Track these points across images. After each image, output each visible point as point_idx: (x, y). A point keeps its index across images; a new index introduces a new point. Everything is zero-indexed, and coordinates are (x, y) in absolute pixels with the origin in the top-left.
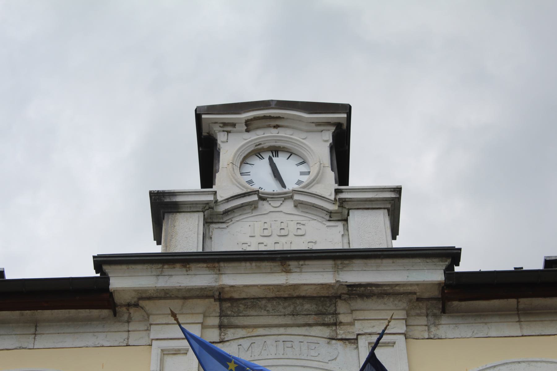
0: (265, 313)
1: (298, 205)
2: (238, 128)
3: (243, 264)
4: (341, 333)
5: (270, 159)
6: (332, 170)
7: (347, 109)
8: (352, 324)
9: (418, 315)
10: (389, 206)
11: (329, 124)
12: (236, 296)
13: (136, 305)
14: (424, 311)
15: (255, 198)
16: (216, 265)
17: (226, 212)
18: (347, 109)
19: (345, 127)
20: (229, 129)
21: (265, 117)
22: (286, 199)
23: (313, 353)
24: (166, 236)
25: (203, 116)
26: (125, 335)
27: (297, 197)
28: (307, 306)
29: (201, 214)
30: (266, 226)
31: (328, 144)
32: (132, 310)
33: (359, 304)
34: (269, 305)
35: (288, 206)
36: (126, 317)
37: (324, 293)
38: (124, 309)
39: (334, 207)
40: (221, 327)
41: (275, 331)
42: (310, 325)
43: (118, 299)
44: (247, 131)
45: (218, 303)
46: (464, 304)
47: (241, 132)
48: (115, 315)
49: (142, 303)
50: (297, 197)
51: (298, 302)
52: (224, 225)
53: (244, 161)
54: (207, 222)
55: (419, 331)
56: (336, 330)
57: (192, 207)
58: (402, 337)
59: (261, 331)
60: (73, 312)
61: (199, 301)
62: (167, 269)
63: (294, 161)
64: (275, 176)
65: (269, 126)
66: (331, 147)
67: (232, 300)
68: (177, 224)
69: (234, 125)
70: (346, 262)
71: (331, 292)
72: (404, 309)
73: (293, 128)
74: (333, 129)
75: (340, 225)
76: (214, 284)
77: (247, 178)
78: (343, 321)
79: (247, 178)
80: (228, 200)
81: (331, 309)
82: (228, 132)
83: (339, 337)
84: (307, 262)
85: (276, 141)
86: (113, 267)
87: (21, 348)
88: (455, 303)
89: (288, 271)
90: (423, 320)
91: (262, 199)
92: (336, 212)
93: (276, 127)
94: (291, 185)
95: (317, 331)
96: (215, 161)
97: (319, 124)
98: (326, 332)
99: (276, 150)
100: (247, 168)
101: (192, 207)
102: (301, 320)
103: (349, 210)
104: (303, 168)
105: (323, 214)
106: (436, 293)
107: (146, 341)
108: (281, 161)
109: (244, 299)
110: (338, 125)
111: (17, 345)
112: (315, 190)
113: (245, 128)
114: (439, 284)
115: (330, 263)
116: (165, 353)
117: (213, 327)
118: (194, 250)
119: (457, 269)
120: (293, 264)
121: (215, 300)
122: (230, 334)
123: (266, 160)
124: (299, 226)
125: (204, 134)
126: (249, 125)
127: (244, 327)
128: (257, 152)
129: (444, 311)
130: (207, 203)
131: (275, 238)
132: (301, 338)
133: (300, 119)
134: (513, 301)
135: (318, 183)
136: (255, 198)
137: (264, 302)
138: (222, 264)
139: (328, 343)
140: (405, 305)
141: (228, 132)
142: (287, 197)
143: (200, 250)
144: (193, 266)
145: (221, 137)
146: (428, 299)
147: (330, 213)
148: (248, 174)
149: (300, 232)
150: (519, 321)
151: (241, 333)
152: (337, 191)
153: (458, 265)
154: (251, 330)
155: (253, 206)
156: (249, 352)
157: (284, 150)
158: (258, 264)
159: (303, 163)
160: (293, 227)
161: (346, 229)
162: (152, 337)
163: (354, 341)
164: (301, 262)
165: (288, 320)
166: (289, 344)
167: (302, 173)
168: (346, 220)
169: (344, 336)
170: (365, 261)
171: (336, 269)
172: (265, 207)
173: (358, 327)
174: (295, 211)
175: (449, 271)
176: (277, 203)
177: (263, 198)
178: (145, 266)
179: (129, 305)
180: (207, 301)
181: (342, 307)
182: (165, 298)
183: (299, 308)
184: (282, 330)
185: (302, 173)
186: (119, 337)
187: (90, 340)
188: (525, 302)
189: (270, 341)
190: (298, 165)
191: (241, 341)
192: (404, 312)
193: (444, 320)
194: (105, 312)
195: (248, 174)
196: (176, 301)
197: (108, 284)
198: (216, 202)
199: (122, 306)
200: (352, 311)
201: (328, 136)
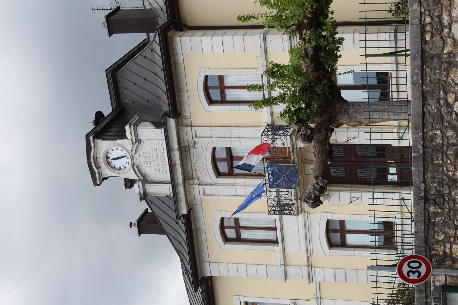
5: (112, 159)
35: (136, 156)
41: (193, 164)
44: (100, 168)
59: (193, 167)
65: (97, 160)
69: (99, 173)
74: (96, 140)
82: (102, 174)
85: (104, 158)
93: (97, 158)
97: (94, 145)
99: (107, 158)
116: (204, 195)
122: (195, 176)
126: (98, 167)
128: (109, 164)
149: (148, 152)
151: (194, 173)
177: (133, 164)
184: (192, 162)
189: (196, 165)
197: (185, 214)
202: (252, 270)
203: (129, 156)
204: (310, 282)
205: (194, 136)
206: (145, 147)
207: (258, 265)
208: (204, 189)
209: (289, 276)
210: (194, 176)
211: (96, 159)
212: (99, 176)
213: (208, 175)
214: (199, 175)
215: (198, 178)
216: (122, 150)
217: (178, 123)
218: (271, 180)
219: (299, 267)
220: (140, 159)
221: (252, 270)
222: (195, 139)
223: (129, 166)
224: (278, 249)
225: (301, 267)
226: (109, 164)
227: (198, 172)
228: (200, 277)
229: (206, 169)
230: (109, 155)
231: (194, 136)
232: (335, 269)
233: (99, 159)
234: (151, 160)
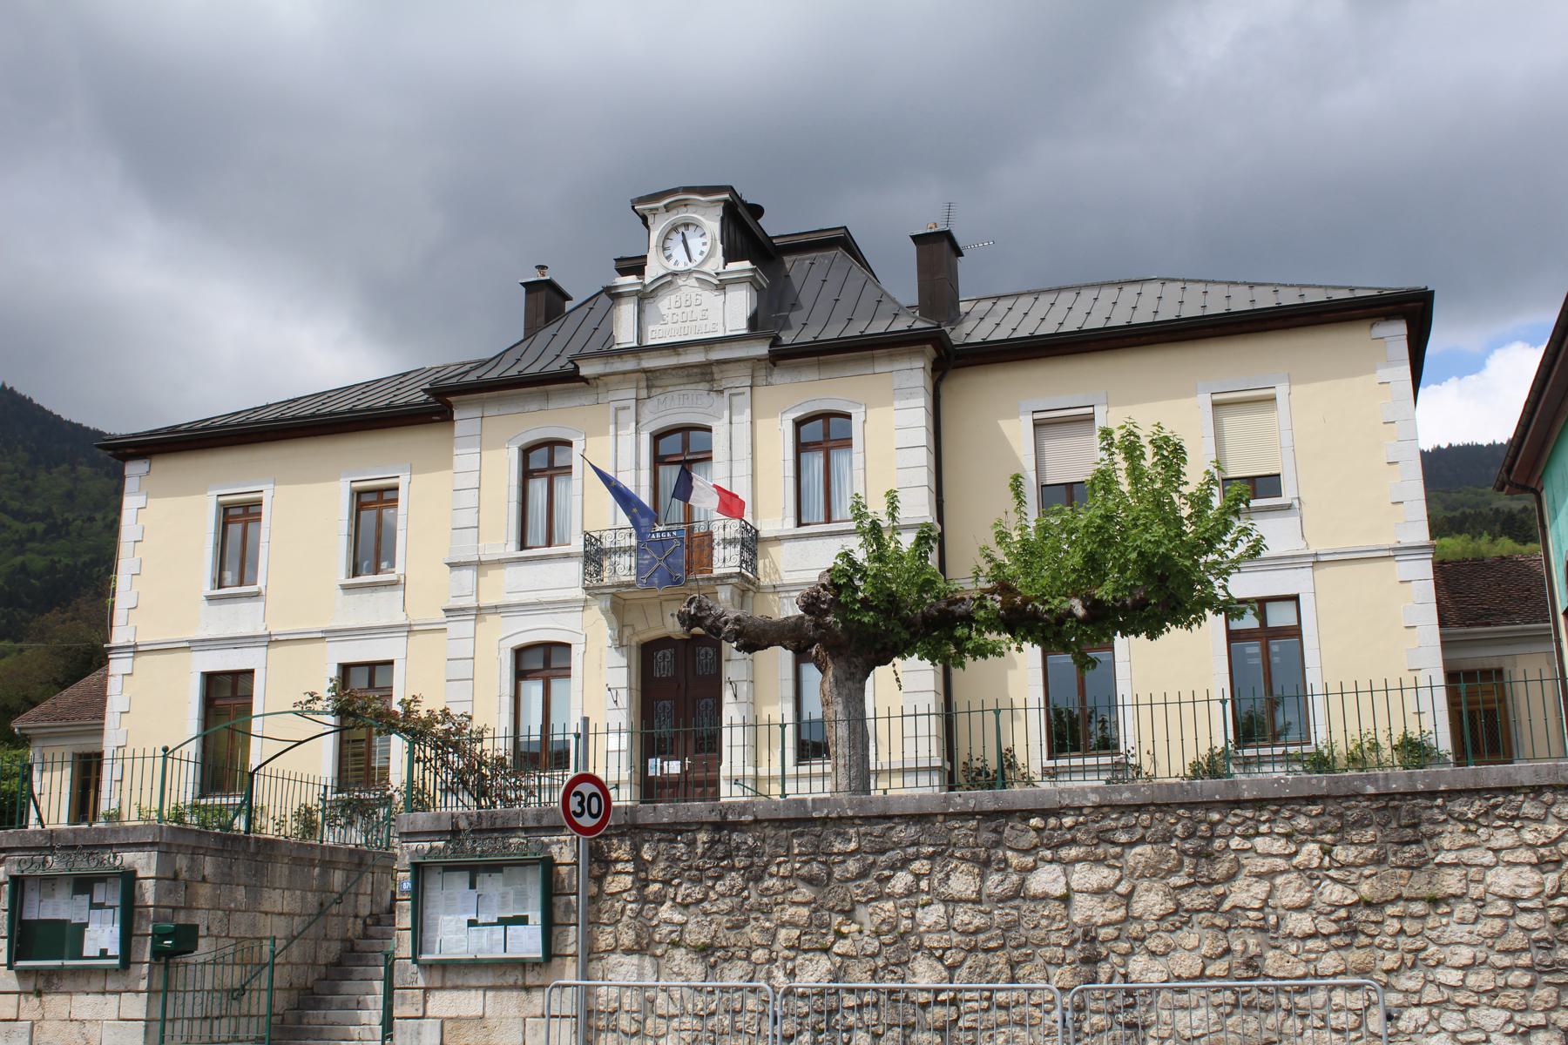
1: (697, 279)
5: (683, 233)
6: (722, 243)
11: (718, 201)
17: (653, 290)
29: (636, 298)
31: (719, 218)
35: (692, 282)
40: (649, 387)
41: (678, 388)
44: (667, 211)
52: (651, 300)
59: (670, 389)
62: (610, 360)
63: (699, 232)
69: (657, 209)
74: (722, 204)
80: (652, 282)
89: (679, 354)
93: (686, 205)
99: (687, 225)
101: (630, 294)
104: (703, 240)
110: (725, 201)
112: (706, 268)
122: (654, 392)
126: (667, 208)
128: (675, 228)
137: (669, 371)
151: (659, 391)
155: (670, 283)
157: (693, 224)
160: (693, 295)
172: (680, 281)
177: (675, 274)
184: (682, 387)
185: (704, 244)
186: (592, 398)
189: (675, 395)
190: (701, 236)
194: (583, 384)
202: (469, 499)
203: (690, 266)
205: (734, 391)
206: (711, 299)
207: (478, 511)
208: (629, 408)
210: (653, 390)
211: (685, 204)
212: (651, 210)
213: (656, 416)
214: (655, 399)
215: (649, 398)
216: (702, 253)
217: (758, 360)
218: (653, 536)
220: (688, 287)
221: (469, 499)
222: (726, 393)
223: (671, 267)
224: (512, 550)
226: (675, 228)
227: (662, 398)
228: (450, 399)
229: (669, 412)
230: (692, 228)
231: (734, 391)
233: (684, 209)
234: (683, 309)
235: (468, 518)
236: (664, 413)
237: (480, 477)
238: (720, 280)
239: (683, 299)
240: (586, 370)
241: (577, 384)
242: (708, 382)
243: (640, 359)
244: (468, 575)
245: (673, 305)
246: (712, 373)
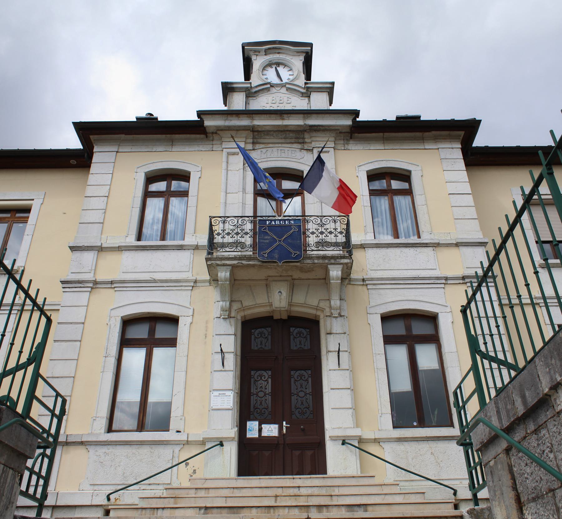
0: (273, 137)
1: (288, 89)
2: (261, 53)
3: (263, 115)
4: (306, 147)
5: (276, 68)
6: (304, 74)
7: (311, 45)
8: (311, 143)
9: (340, 139)
10: (329, 91)
11: (303, 52)
12: (260, 129)
13: (216, 133)
14: (343, 138)
15: (269, 86)
16: (251, 115)
17: (256, 92)
18: (311, 45)
19: (310, 54)
20: (257, 54)
21: (274, 48)
22: (282, 86)
23: (293, 155)
24: (229, 102)
25: (246, 47)
26: (211, 146)
27: (287, 86)
28: (291, 135)
29: (244, 93)
30: (273, 99)
31: (302, 62)
32: (214, 135)
33: (314, 134)
34: (275, 134)
35: (284, 90)
36: (211, 138)
37: (299, 129)
38: (211, 135)
39: (304, 91)
41: (277, 145)
42: (292, 143)
43: (208, 130)
44: (265, 55)
45: (252, 133)
46: (360, 135)
47: (262, 55)
48: (207, 137)
49: (218, 132)
50: (287, 86)
51: (287, 133)
52: (255, 98)
53: (264, 69)
54: (247, 97)
55: (339, 147)
56: (304, 146)
57: (240, 90)
58: (333, 149)
59: (271, 145)
60: (188, 135)
61: (244, 132)
62: (230, 117)
63: (286, 69)
64: (278, 76)
65: (275, 53)
66: (303, 63)
67: (258, 131)
68: (234, 97)
70: (309, 115)
71: (302, 129)
72: (334, 137)
73: (286, 54)
74: (304, 54)
75: (307, 99)
76: (250, 124)
77: (265, 77)
78: (307, 141)
79: (265, 77)
80: (257, 87)
81: (302, 136)
82: (257, 55)
83: (305, 148)
84: (291, 115)
85: (279, 60)
86: (206, 116)
87: (166, 151)
88: (356, 134)
89: (283, 119)
90: (342, 142)
91: (272, 86)
92: (305, 93)
93: (279, 53)
94: (285, 80)
95: (295, 146)
96: (251, 69)
98: (300, 146)
99: (278, 64)
100: (265, 72)
101: (240, 90)
102: (288, 141)
103: (311, 92)
104: (291, 73)
105: (299, 94)
106: (348, 130)
107: (221, 149)
108: (280, 69)
109: (264, 131)
110: (307, 53)
111: (165, 150)
112: (296, 83)
113: (265, 53)
114: (350, 126)
115: (302, 115)
116: (229, 154)
117: (250, 143)
118: (242, 109)
119: (358, 119)
120: (285, 116)
121: (251, 131)
122: (257, 146)
123: (274, 69)
124: (288, 99)
125: (246, 56)
126: (267, 52)
127: (263, 143)
128: (270, 65)
129: (351, 138)
130: (247, 88)
131: (277, 104)
132: (288, 149)
133: (290, 49)
134: (381, 134)
135: (297, 79)
136: (269, 86)
137: (272, 132)
138: (254, 115)
139: (300, 151)
140: (334, 135)
141: (257, 55)
142: (283, 86)
143: (244, 109)
144: (241, 116)
145: (253, 58)
146: (344, 133)
147: (302, 93)
148: (265, 75)
149: (289, 102)
150: (384, 143)
152: (306, 84)
153: (358, 118)
154: (266, 145)
155: (268, 90)
156: (266, 154)
158: (270, 115)
159: (291, 70)
160: (285, 99)
161: (309, 100)
162: (223, 147)
163: (311, 150)
164: (289, 115)
165: (283, 141)
166: (283, 151)
167: (290, 75)
168: (309, 97)
169: (307, 148)
170: (318, 115)
171: (304, 119)
172: (273, 90)
173: (313, 144)
174: (286, 92)
175: (354, 120)
176: (279, 89)
177: (272, 86)
178: (219, 116)
179: (213, 133)
180: (247, 132)
181: (306, 135)
182: (229, 130)
183: (288, 136)
184: (280, 145)
185: (290, 75)
186: (209, 147)
187: (197, 148)
188: (386, 135)
189: (275, 149)
190: (288, 71)
191: (262, 150)
192: (334, 138)
193: (351, 142)
195: (265, 75)
196: (234, 131)
197: (204, 123)
198: (251, 87)
199: (210, 133)
200: (311, 137)
201: (302, 58)
204: (63, 282)
207: (105, 213)
209: (78, 254)
211: (277, 51)
212: (255, 51)
214: (259, 151)
215: (254, 150)
219: (93, 268)
224: (131, 240)
225: (93, 272)
227: (264, 150)
229: (269, 159)
232: (83, 323)
235: (96, 216)
236: (265, 160)
237: (110, 189)
238: (308, 88)
239: (278, 99)
240: (209, 123)
241: (198, 136)
242: (300, 143)
243: (253, 119)
244: (89, 257)
245: (270, 102)
246: (304, 138)
